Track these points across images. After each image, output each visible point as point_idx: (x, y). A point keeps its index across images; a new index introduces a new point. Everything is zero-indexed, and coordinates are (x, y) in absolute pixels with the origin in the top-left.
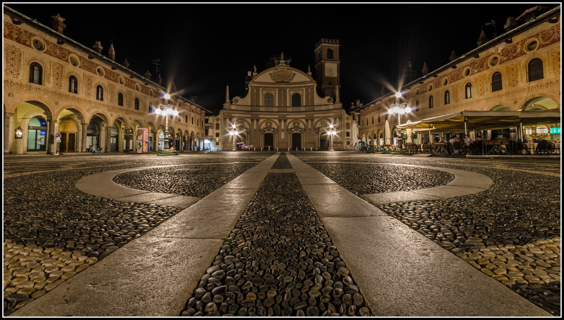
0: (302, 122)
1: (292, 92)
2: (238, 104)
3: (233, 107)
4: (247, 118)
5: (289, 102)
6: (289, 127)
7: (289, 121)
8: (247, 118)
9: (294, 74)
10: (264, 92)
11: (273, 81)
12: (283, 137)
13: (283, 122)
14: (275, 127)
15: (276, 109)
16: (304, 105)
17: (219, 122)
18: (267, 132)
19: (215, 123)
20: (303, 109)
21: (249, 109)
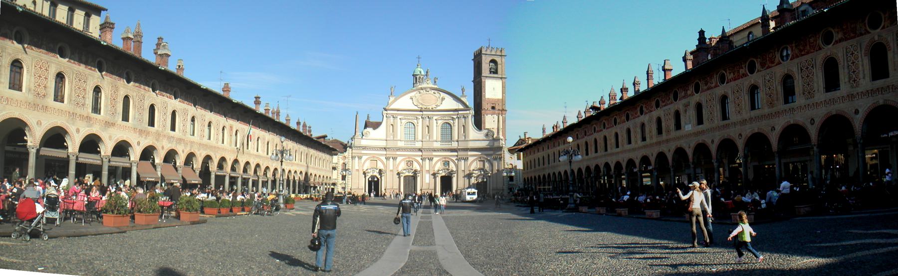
0: (453, 161)
1: (440, 122)
2: (370, 137)
3: (364, 143)
4: (382, 155)
5: (436, 132)
6: (436, 169)
7: (435, 159)
8: (382, 155)
9: (443, 99)
10: (403, 121)
11: (416, 108)
12: (427, 181)
13: (427, 161)
14: (418, 168)
15: (418, 145)
16: (456, 138)
17: (346, 161)
18: (407, 174)
19: (341, 162)
20: (455, 145)
21: (383, 144)
